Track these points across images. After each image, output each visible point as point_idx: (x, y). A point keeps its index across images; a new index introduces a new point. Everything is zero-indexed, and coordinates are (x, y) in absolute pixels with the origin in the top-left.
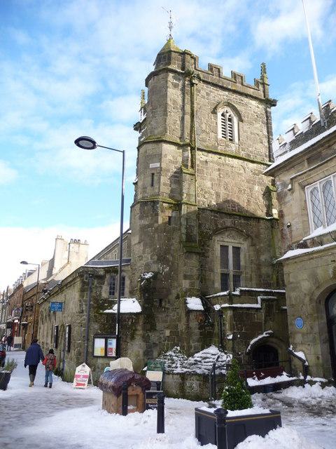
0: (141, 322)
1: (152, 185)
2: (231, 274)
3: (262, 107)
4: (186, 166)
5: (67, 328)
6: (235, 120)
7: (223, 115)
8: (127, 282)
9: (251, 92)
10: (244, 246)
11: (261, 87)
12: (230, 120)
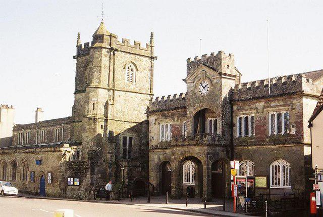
0: (90, 171)
1: (94, 109)
2: (128, 149)
3: (149, 61)
4: (110, 100)
5: (50, 174)
6: (134, 70)
7: (128, 68)
8: (81, 154)
9: (143, 53)
10: (134, 136)
11: (150, 48)
12: (132, 70)
